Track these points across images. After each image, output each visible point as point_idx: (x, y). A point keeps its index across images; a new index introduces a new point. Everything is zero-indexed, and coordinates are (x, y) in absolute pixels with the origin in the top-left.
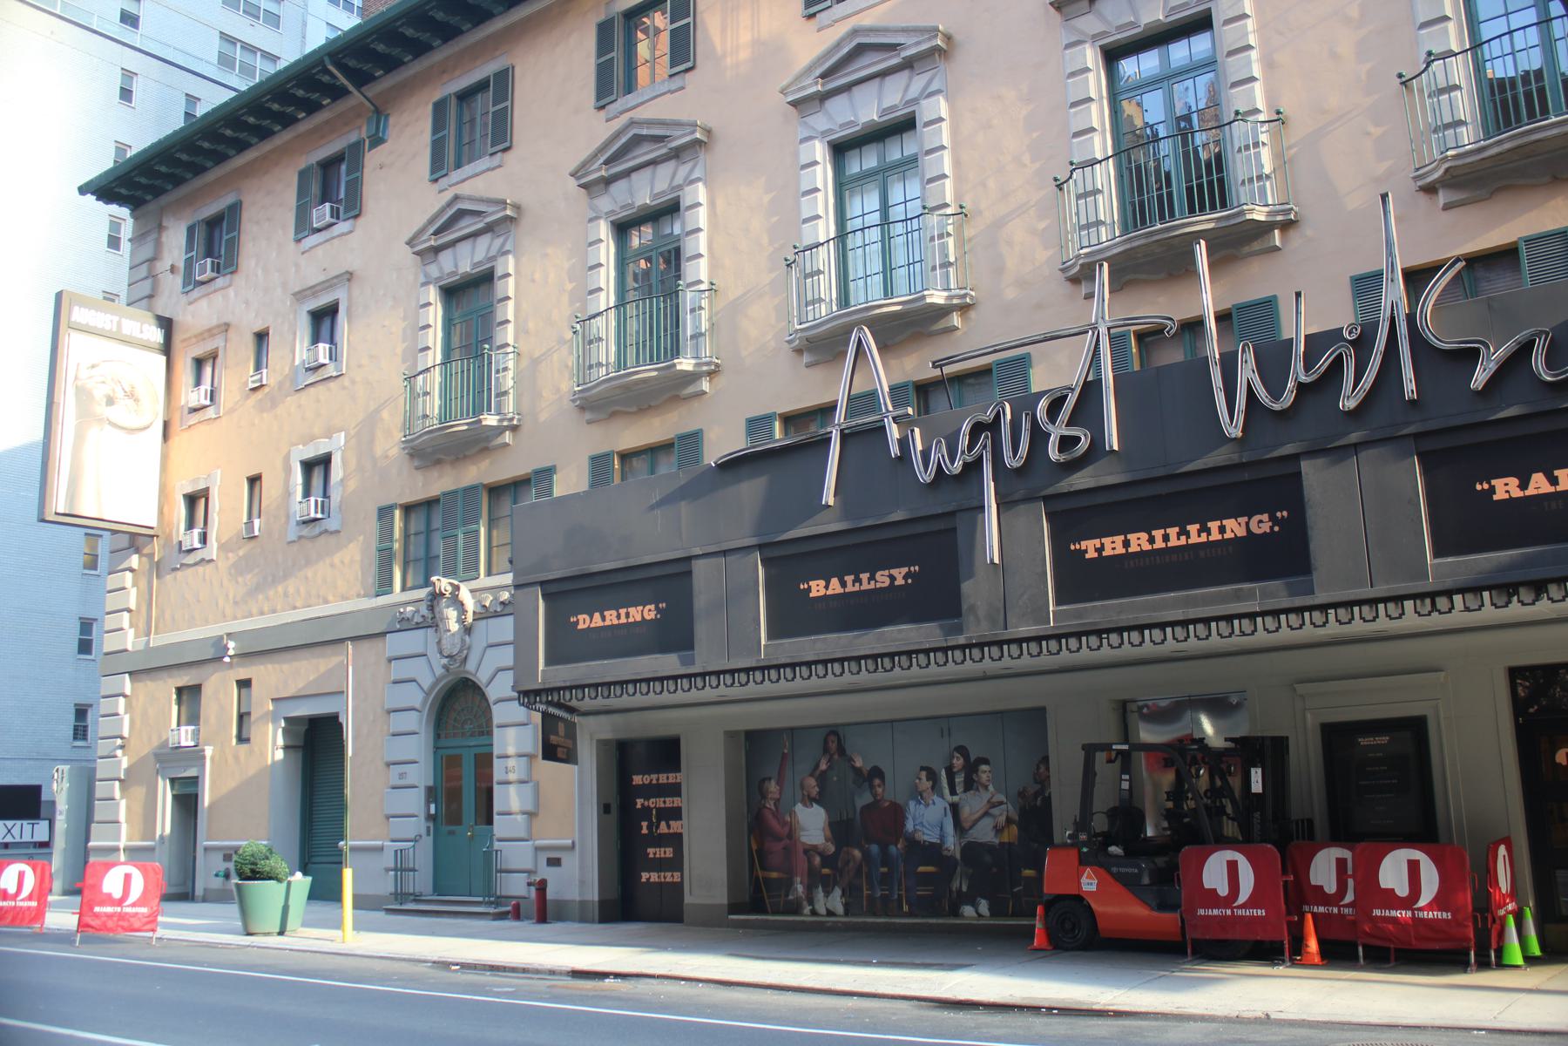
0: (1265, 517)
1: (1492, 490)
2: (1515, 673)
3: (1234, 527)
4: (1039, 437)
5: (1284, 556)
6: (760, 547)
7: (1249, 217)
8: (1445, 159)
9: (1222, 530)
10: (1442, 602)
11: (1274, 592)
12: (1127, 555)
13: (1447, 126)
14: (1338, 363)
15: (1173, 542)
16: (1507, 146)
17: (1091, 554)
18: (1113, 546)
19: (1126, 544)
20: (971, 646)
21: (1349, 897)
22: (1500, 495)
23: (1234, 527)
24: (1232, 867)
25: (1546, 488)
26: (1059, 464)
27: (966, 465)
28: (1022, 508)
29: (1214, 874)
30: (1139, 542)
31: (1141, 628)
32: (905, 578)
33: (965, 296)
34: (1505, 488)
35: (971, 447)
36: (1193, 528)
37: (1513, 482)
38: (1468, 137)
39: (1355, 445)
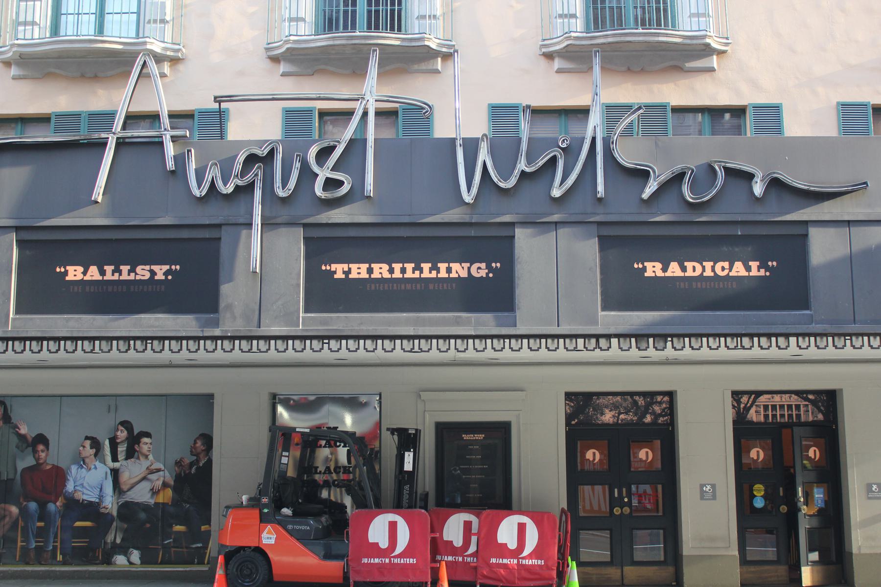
0: (483, 265)
1: (644, 269)
2: (569, 396)
3: (459, 270)
4: (307, 175)
5: (495, 295)
6: (17, 229)
7: (427, 43)
8: (569, 38)
9: (449, 270)
10: (603, 342)
11: (486, 322)
12: (370, 280)
13: (566, 16)
14: (553, 161)
15: (409, 274)
16: (610, 40)
17: (339, 275)
18: (359, 271)
19: (370, 271)
20: (222, 338)
21: (472, 549)
22: (649, 273)
23: (459, 270)
24: (393, 526)
25: (679, 273)
26: (320, 199)
27: (237, 187)
28: (283, 230)
29: (378, 531)
30: (381, 270)
31: (375, 338)
32: (166, 274)
33: (178, 50)
34: (653, 269)
35: (243, 173)
36: (426, 266)
37: (659, 265)
38: (578, 26)
39: (556, 223)
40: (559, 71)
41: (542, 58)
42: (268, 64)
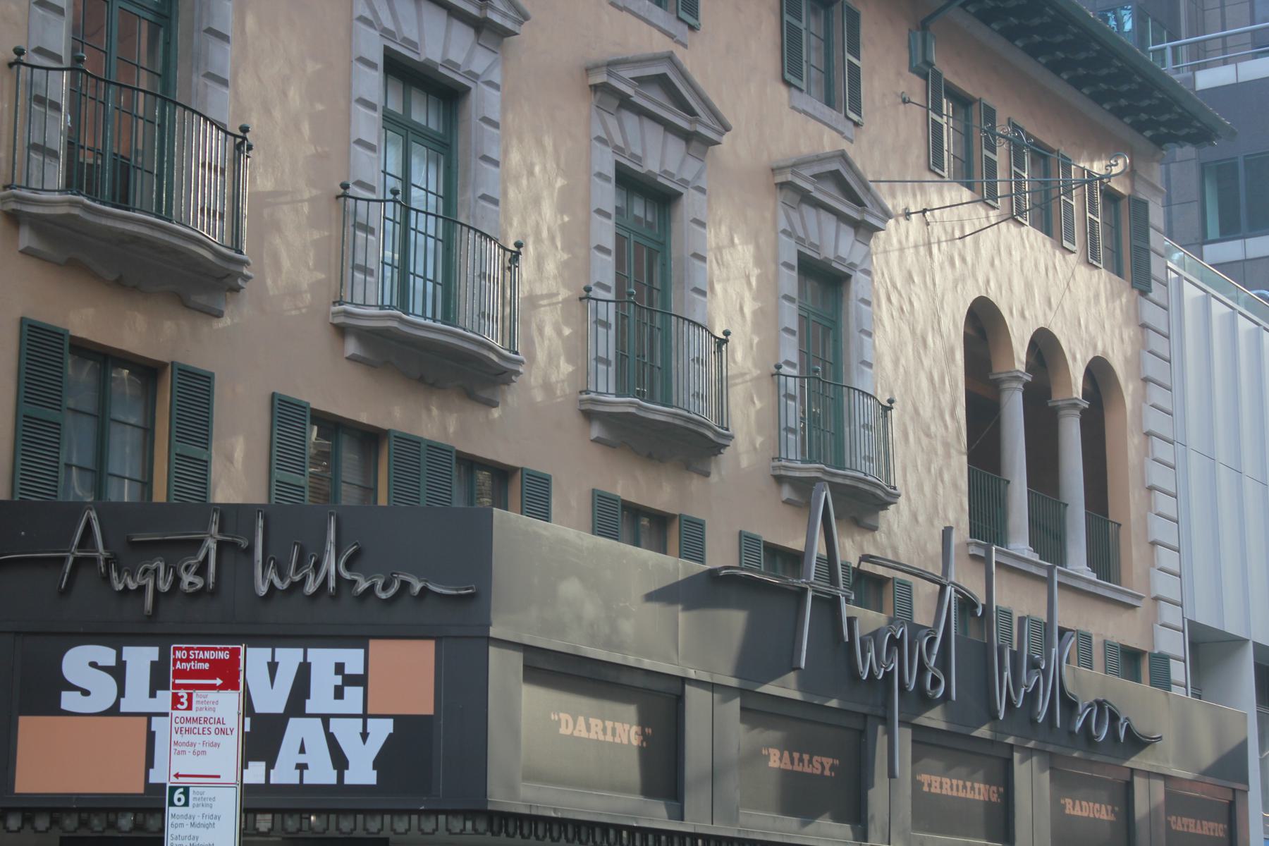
4: (922, 669)
15: (962, 794)
17: (926, 789)
32: (832, 768)
39: (1031, 749)
40: (787, 502)
41: (772, 480)
42: (578, 421)
